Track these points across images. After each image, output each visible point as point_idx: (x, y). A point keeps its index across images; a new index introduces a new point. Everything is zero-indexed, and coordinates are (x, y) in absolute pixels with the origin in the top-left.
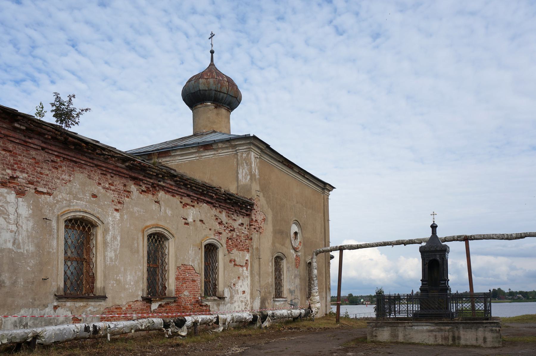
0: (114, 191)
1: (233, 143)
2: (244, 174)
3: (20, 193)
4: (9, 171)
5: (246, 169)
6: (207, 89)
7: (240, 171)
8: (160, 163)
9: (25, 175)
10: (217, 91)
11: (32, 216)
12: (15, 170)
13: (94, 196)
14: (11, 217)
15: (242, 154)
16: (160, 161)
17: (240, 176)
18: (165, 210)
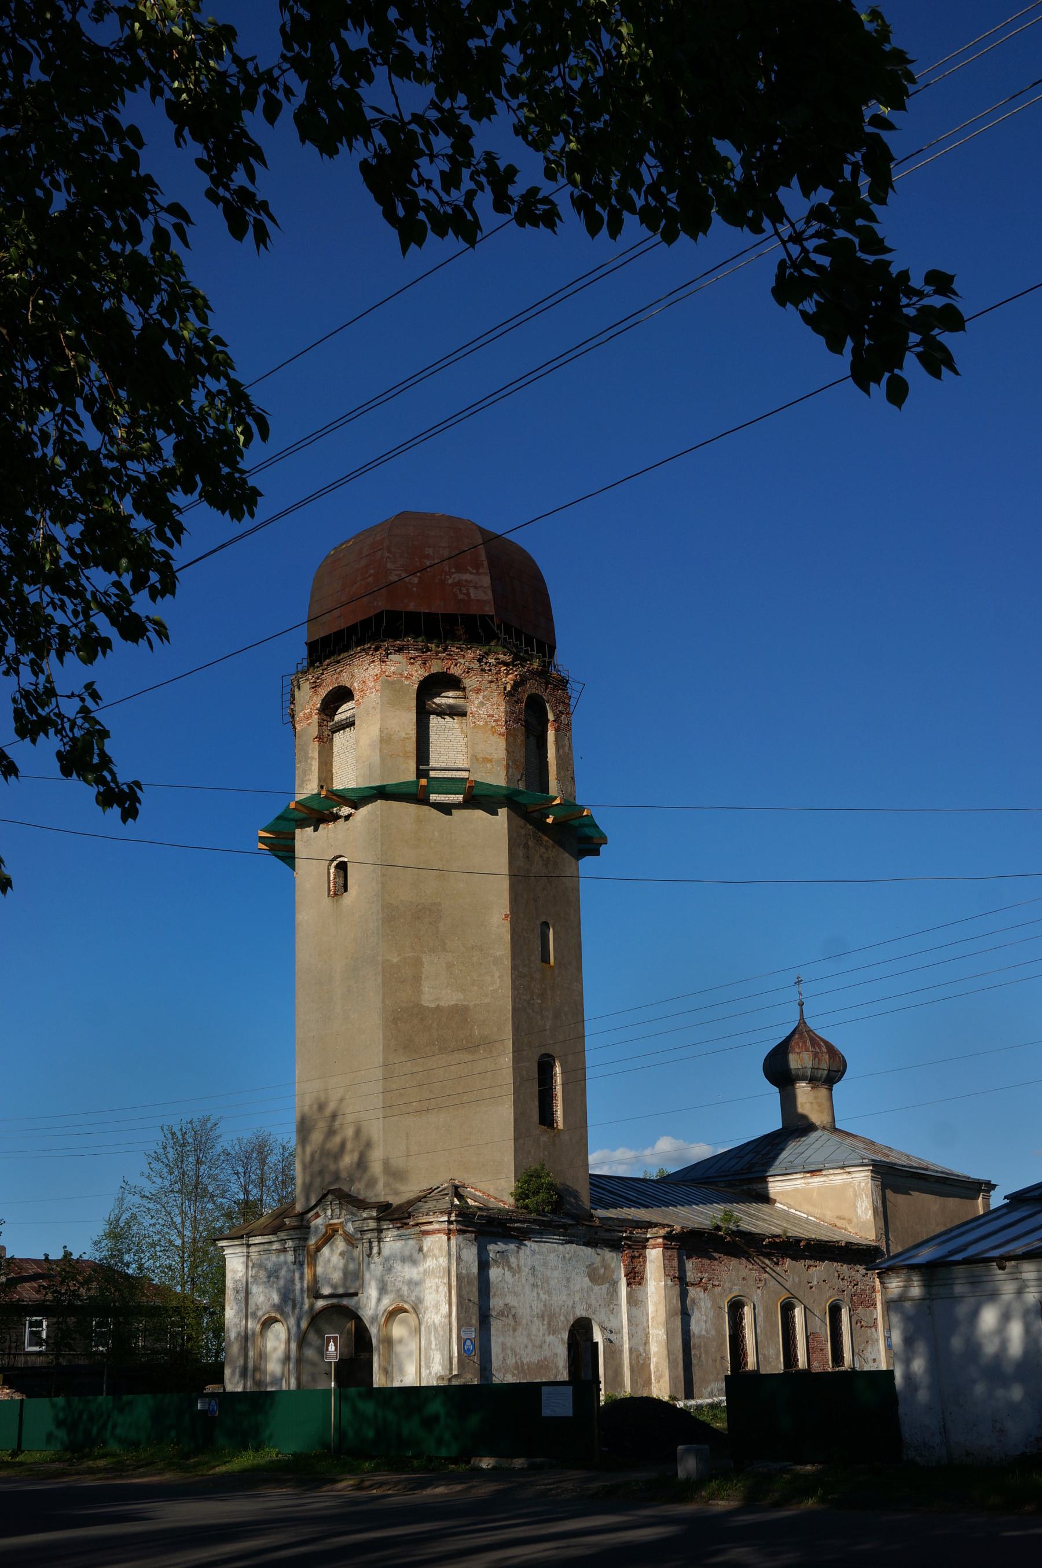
0: (756, 1270)
1: (848, 1170)
2: (863, 1209)
3: (705, 1290)
4: (699, 1274)
5: (865, 1202)
6: (800, 1067)
7: (859, 1205)
8: (755, 1190)
9: (707, 1274)
10: (814, 1068)
11: (713, 1306)
12: (702, 1272)
13: (744, 1279)
14: (703, 1309)
15: (860, 1182)
16: (755, 1187)
17: (859, 1212)
18: (793, 1278)
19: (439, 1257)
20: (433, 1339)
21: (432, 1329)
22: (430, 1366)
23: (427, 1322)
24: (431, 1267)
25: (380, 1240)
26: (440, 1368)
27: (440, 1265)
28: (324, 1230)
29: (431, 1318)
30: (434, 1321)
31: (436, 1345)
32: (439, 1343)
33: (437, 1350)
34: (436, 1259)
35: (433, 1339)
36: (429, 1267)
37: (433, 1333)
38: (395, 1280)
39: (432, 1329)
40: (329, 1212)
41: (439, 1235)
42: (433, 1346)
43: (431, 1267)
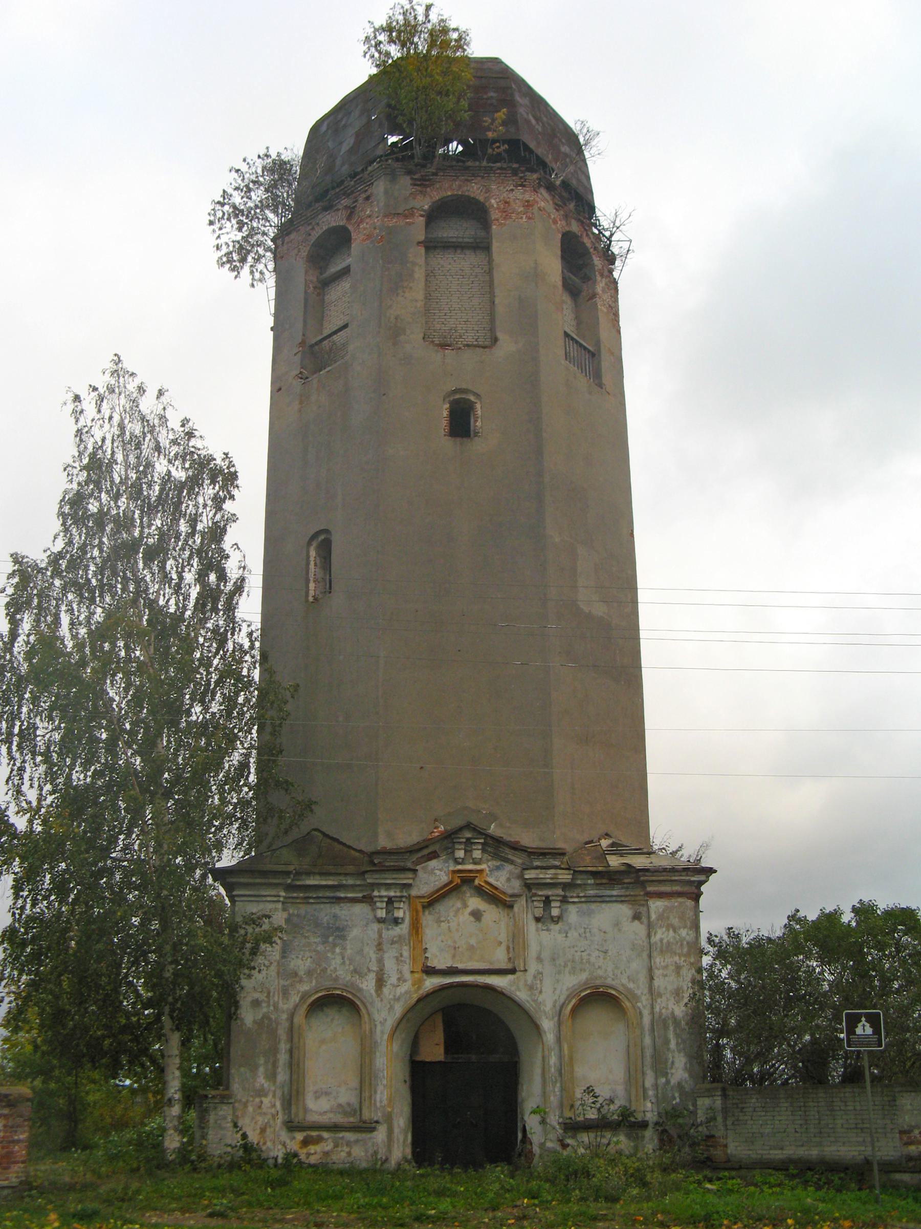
19: (680, 928)
20: (671, 1035)
21: (670, 1022)
22: (667, 1073)
23: (661, 1014)
24: (665, 941)
25: (564, 900)
26: (686, 1075)
27: (682, 940)
28: (445, 879)
29: (667, 1009)
30: (673, 1013)
31: (677, 1044)
32: (684, 1041)
33: (679, 1052)
34: (675, 931)
35: (671, 1035)
36: (661, 940)
37: (671, 1028)
38: (589, 955)
39: (670, 1022)
40: (460, 854)
41: (680, 900)
42: (673, 1044)
43: (665, 941)
